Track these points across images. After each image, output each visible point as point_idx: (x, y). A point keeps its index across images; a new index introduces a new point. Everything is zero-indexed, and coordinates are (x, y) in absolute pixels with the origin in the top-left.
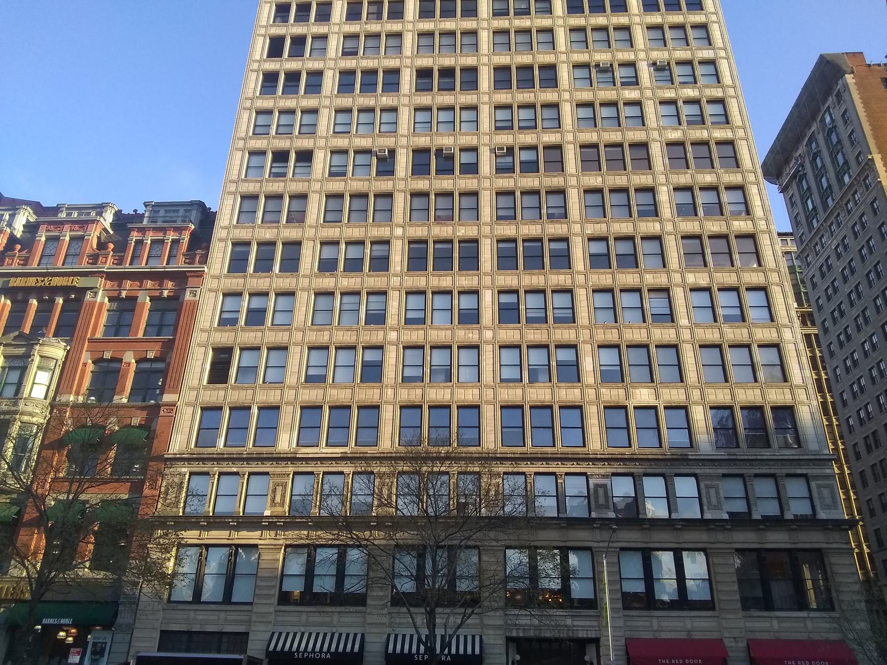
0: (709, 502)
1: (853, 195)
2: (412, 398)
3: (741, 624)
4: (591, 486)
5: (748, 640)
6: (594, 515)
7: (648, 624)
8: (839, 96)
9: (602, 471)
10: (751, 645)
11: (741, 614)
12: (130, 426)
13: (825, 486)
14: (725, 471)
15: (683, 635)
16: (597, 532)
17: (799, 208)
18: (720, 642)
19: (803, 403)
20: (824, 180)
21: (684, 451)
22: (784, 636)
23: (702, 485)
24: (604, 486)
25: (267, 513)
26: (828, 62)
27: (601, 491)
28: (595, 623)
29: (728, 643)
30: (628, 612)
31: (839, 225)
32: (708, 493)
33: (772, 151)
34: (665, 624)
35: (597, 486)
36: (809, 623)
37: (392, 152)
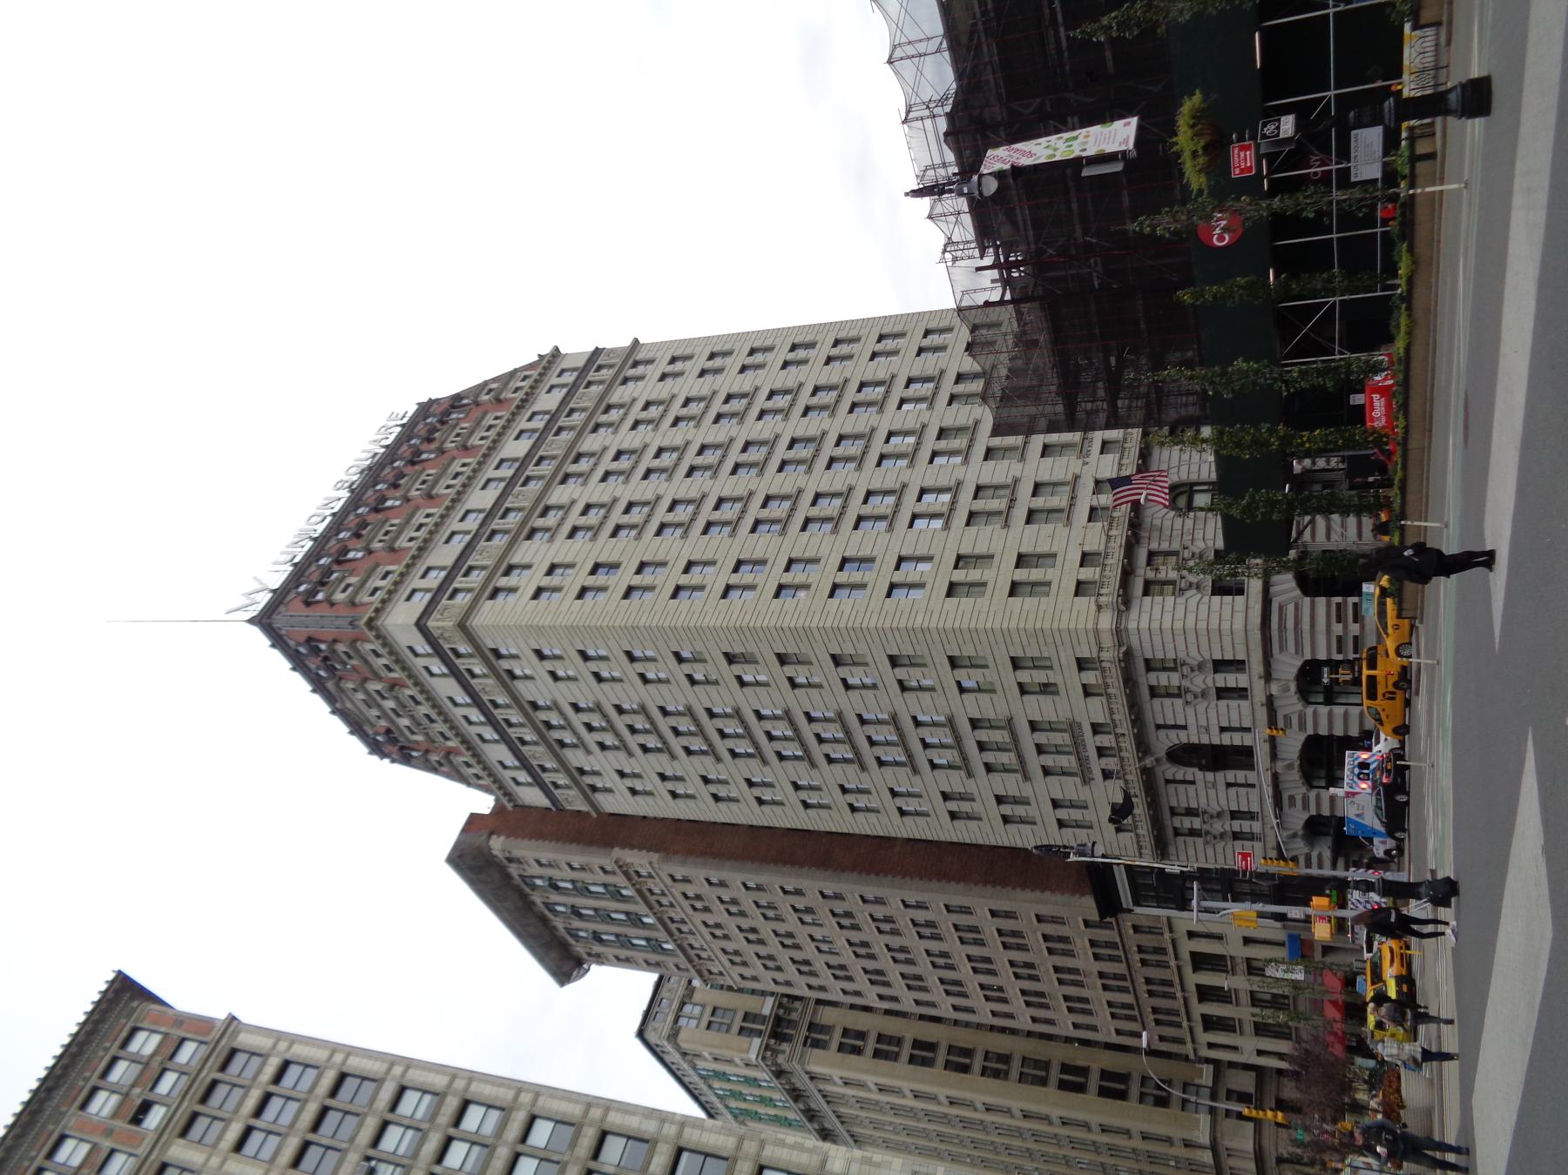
1: (652, 893)
8: (510, 860)
17: (639, 956)
20: (614, 916)
26: (460, 857)
31: (683, 922)
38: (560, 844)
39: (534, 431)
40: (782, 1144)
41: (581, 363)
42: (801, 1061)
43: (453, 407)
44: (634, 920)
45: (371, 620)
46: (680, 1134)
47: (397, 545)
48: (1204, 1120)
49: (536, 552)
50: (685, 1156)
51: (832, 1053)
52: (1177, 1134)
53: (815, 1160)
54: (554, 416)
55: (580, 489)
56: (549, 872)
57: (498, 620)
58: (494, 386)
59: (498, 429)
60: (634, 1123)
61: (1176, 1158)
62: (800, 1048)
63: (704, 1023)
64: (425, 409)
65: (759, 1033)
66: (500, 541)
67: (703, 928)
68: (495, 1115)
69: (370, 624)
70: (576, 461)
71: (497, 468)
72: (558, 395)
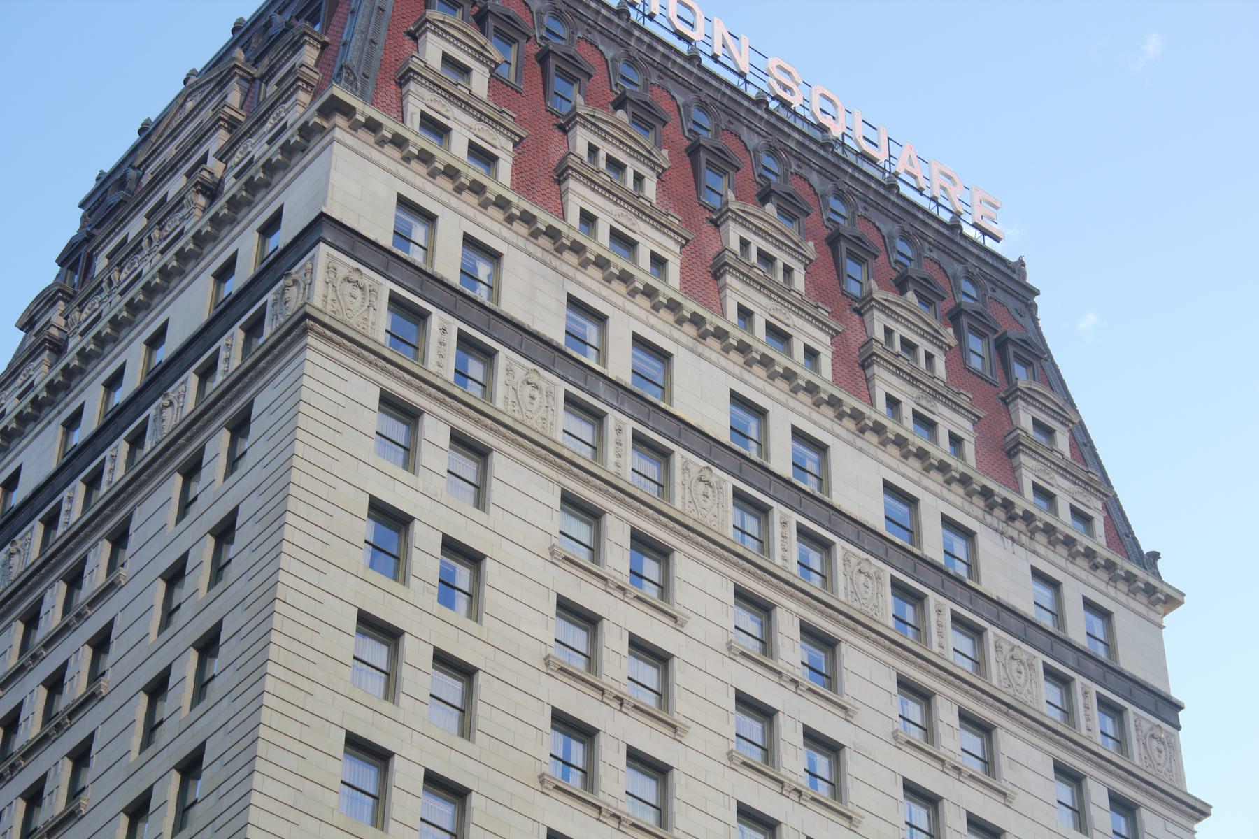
39: (913, 533)
41: (1126, 663)
43: (1001, 345)
45: (348, 111)
47: (572, 184)
49: (521, 516)
54: (960, 585)
55: (719, 639)
57: (329, 411)
58: (1062, 441)
59: (1043, 516)
64: (1010, 282)
66: (561, 426)
69: (334, 107)
70: (967, 719)
71: (948, 522)
72: (1025, 597)
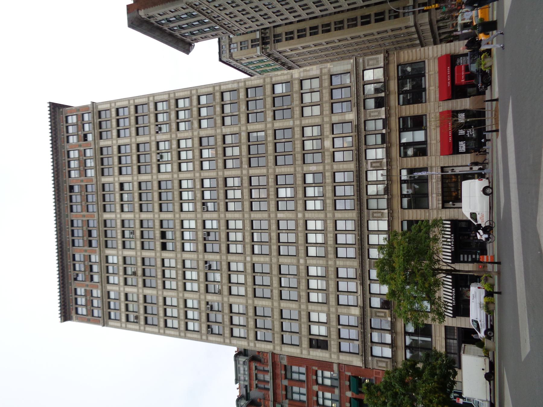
0: (377, 116)
1: (204, 10)
2: (332, 252)
3: (432, 104)
4: (372, 169)
5: (440, 100)
6: (385, 168)
7: (433, 145)
8: (149, 18)
9: (365, 164)
10: (442, 99)
11: (428, 103)
12: (350, 386)
13: (368, 62)
14: (362, 108)
15: (438, 129)
16: (393, 167)
17: (209, 34)
18: (441, 113)
19: (329, 70)
20: (194, 24)
21: (354, 127)
22: (437, 85)
23: (370, 118)
24: (371, 163)
25: (389, 319)
26: (132, 23)
27: (374, 165)
28: (434, 168)
29: (441, 110)
30: (429, 154)
31: (219, 16)
32: (373, 116)
33: (177, 48)
34: (433, 138)
35: (371, 166)
36: (431, 73)
37: (206, 262)
38: (164, 5)
40: (278, 75)
42: (275, 49)
44: (202, 22)
46: (245, 84)
48: (411, 17)
50: (249, 90)
51: (284, 42)
52: (402, 25)
53: (289, 76)
56: (165, 17)
60: (230, 87)
61: (403, 34)
62: (273, 44)
63: (239, 48)
65: (258, 45)
67: (226, 16)
68: (187, 100)
